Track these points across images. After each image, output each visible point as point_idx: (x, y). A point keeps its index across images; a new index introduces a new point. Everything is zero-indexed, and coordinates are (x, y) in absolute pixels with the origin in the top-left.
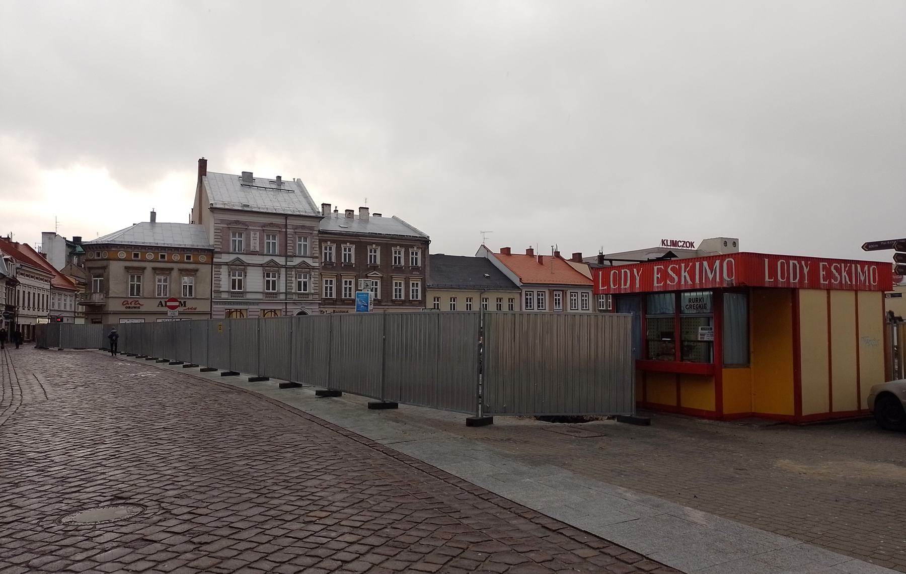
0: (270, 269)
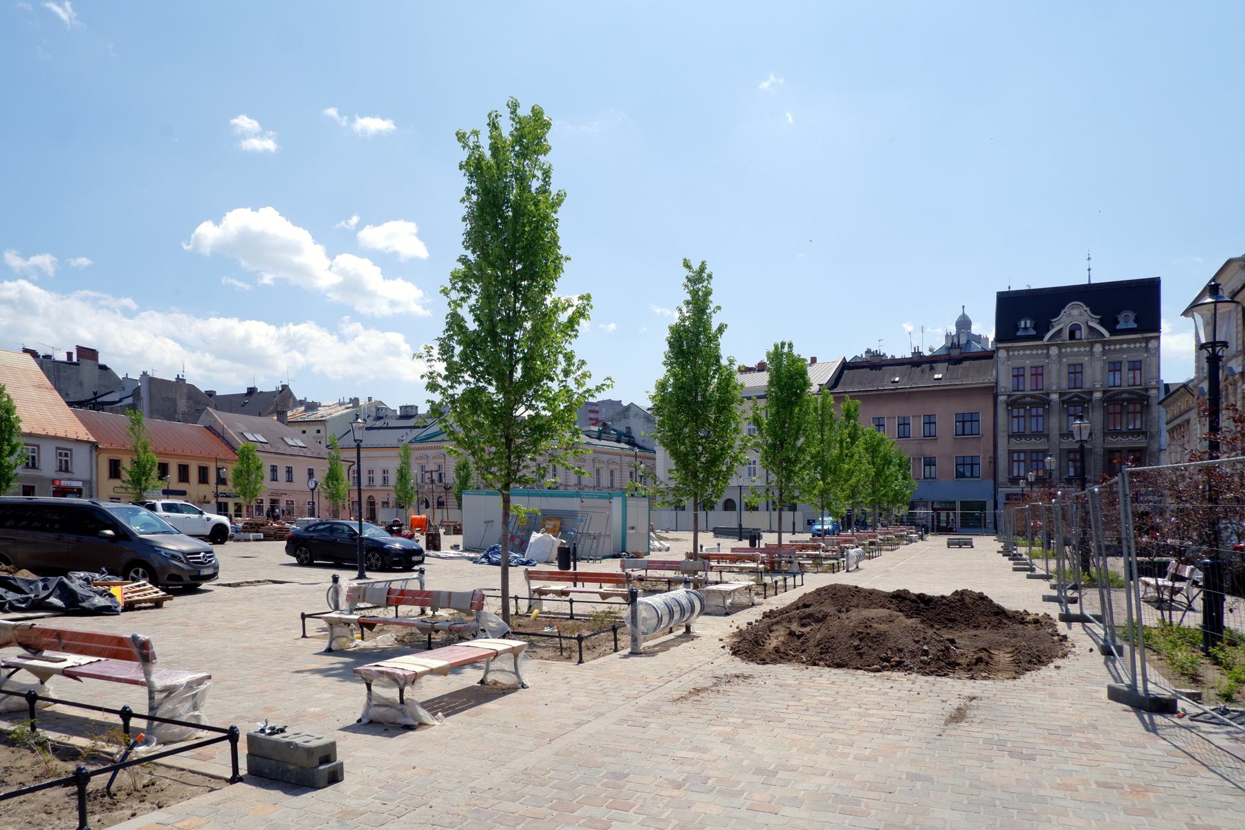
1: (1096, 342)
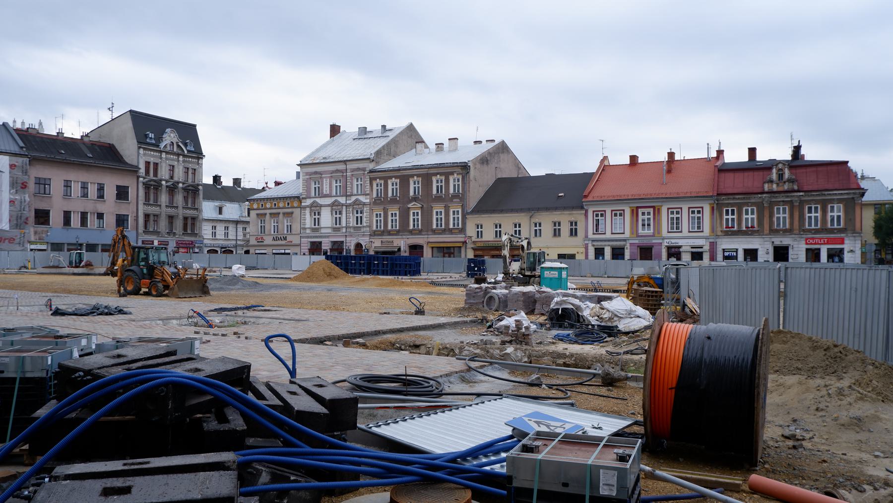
0: (336, 207)
1: (181, 155)
